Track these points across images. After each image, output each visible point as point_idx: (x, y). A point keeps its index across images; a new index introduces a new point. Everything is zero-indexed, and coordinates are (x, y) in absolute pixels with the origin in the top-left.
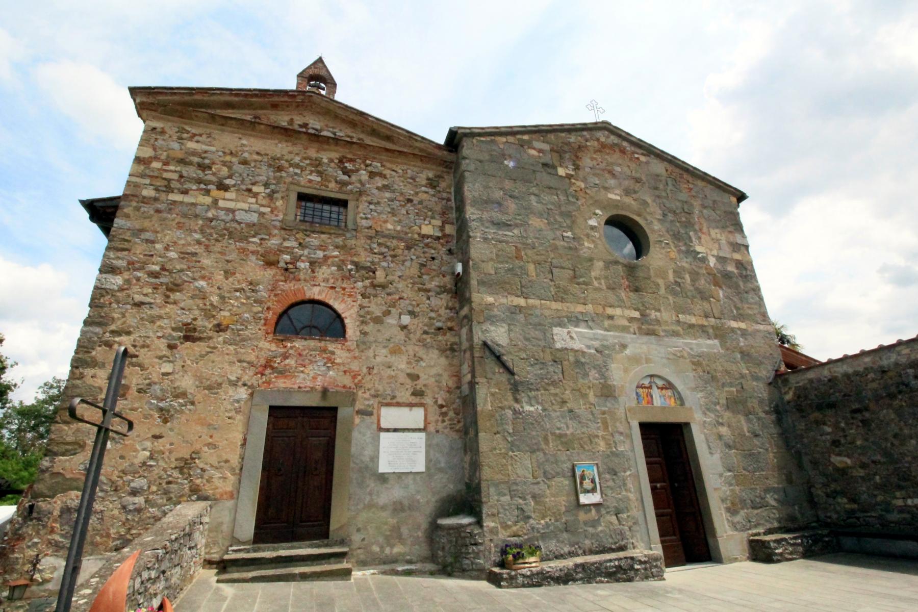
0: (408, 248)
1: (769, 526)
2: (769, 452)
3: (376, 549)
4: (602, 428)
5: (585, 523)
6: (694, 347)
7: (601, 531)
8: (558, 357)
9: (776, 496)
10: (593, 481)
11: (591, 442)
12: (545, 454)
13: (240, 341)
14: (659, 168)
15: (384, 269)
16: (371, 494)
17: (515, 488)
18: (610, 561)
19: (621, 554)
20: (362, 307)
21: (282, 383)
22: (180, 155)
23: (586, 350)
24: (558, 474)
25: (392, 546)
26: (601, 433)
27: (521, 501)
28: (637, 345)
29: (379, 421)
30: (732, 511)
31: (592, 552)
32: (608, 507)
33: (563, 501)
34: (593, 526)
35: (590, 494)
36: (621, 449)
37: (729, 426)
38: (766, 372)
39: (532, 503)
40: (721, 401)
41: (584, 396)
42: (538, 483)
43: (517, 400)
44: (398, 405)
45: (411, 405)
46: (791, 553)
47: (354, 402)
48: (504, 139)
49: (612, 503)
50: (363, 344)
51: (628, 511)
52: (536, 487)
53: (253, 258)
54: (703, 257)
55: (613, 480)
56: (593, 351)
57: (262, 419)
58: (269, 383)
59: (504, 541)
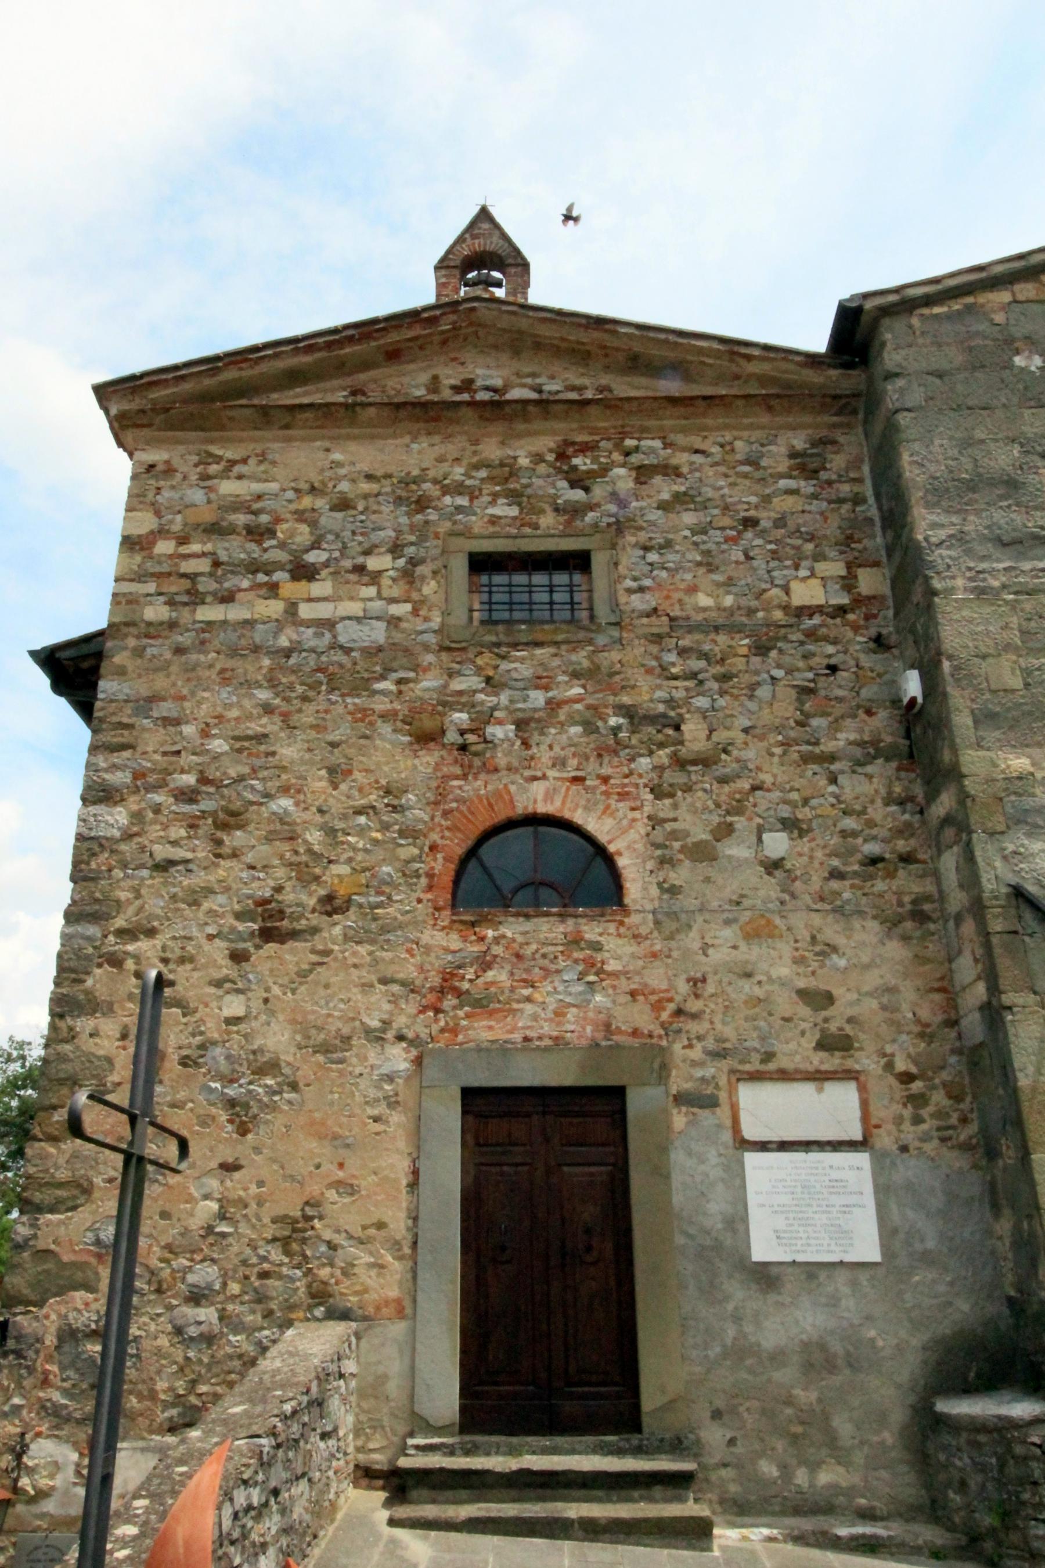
0: (761, 650)
3: (768, 1469)
13: (379, 932)
20: (655, 821)
21: (483, 1031)
22: (208, 516)
25: (814, 1467)
44: (784, 1076)
45: (819, 1077)
47: (663, 1072)
48: (1004, 296)
50: (671, 920)
53: (385, 729)
57: (449, 1117)
58: (454, 1031)
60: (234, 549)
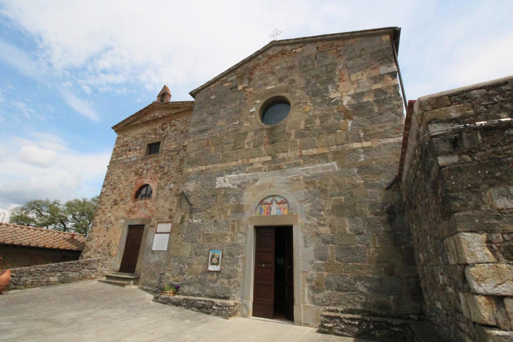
1: (350, 307)
2: (371, 247)
3: (147, 280)
4: (231, 230)
5: (210, 281)
6: (309, 171)
7: (216, 286)
8: (215, 193)
9: (368, 284)
10: (218, 259)
11: (223, 238)
12: (198, 244)
14: (311, 50)
15: (168, 166)
16: (149, 258)
17: (180, 259)
18: (201, 301)
19: (224, 301)
20: (158, 184)
21: (133, 217)
22: (122, 144)
23: (231, 187)
24: (202, 254)
25: (153, 280)
26: (229, 233)
27: (182, 266)
28: (265, 178)
29: (156, 229)
30: (316, 288)
31: (209, 296)
32: (224, 274)
33: (201, 268)
34: (214, 283)
35: (215, 266)
36: (240, 242)
37: (330, 226)
38: (384, 180)
39: (187, 267)
40: (326, 209)
41: (225, 213)
42: (191, 258)
43: (191, 218)
44: (164, 222)
45: (167, 222)
46: (342, 330)
48: (214, 85)
49: (226, 272)
50: (156, 199)
51: (235, 278)
52: (190, 259)
53: (133, 173)
54: (337, 101)
55: (230, 259)
56: (236, 187)
57: (126, 229)
58: (130, 217)
59: (171, 283)
60: (123, 149)
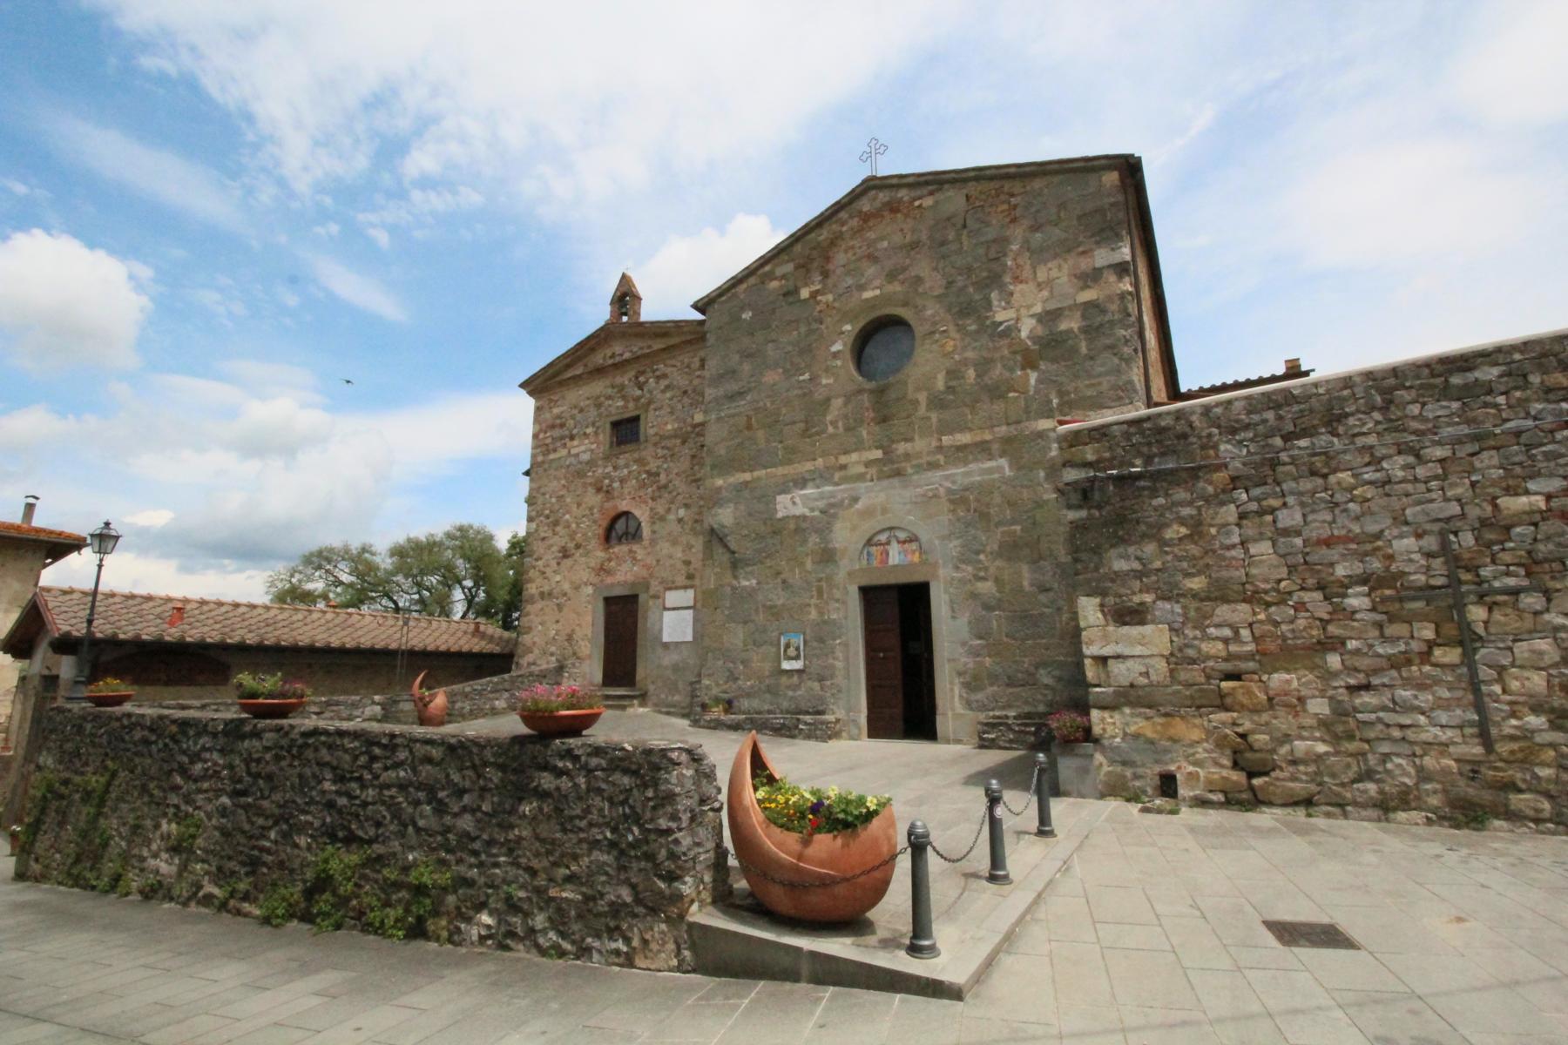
0: (684, 442)
1: (1027, 709)
5: (788, 687)
10: (797, 649)
13: (587, 554)
14: (954, 201)
21: (609, 580)
22: (550, 422)
28: (873, 494)
30: (973, 683)
33: (767, 667)
36: (834, 616)
37: (997, 580)
40: (988, 549)
41: (802, 564)
43: (735, 577)
44: (677, 588)
45: (685, 587)
46: (1011, 741)
47: (648, 588)
48: (744, 286)
50: (653, 542)
54: (1008, 328)
56: (817, 513)
57: (601, 605)
60: (557, 433)
